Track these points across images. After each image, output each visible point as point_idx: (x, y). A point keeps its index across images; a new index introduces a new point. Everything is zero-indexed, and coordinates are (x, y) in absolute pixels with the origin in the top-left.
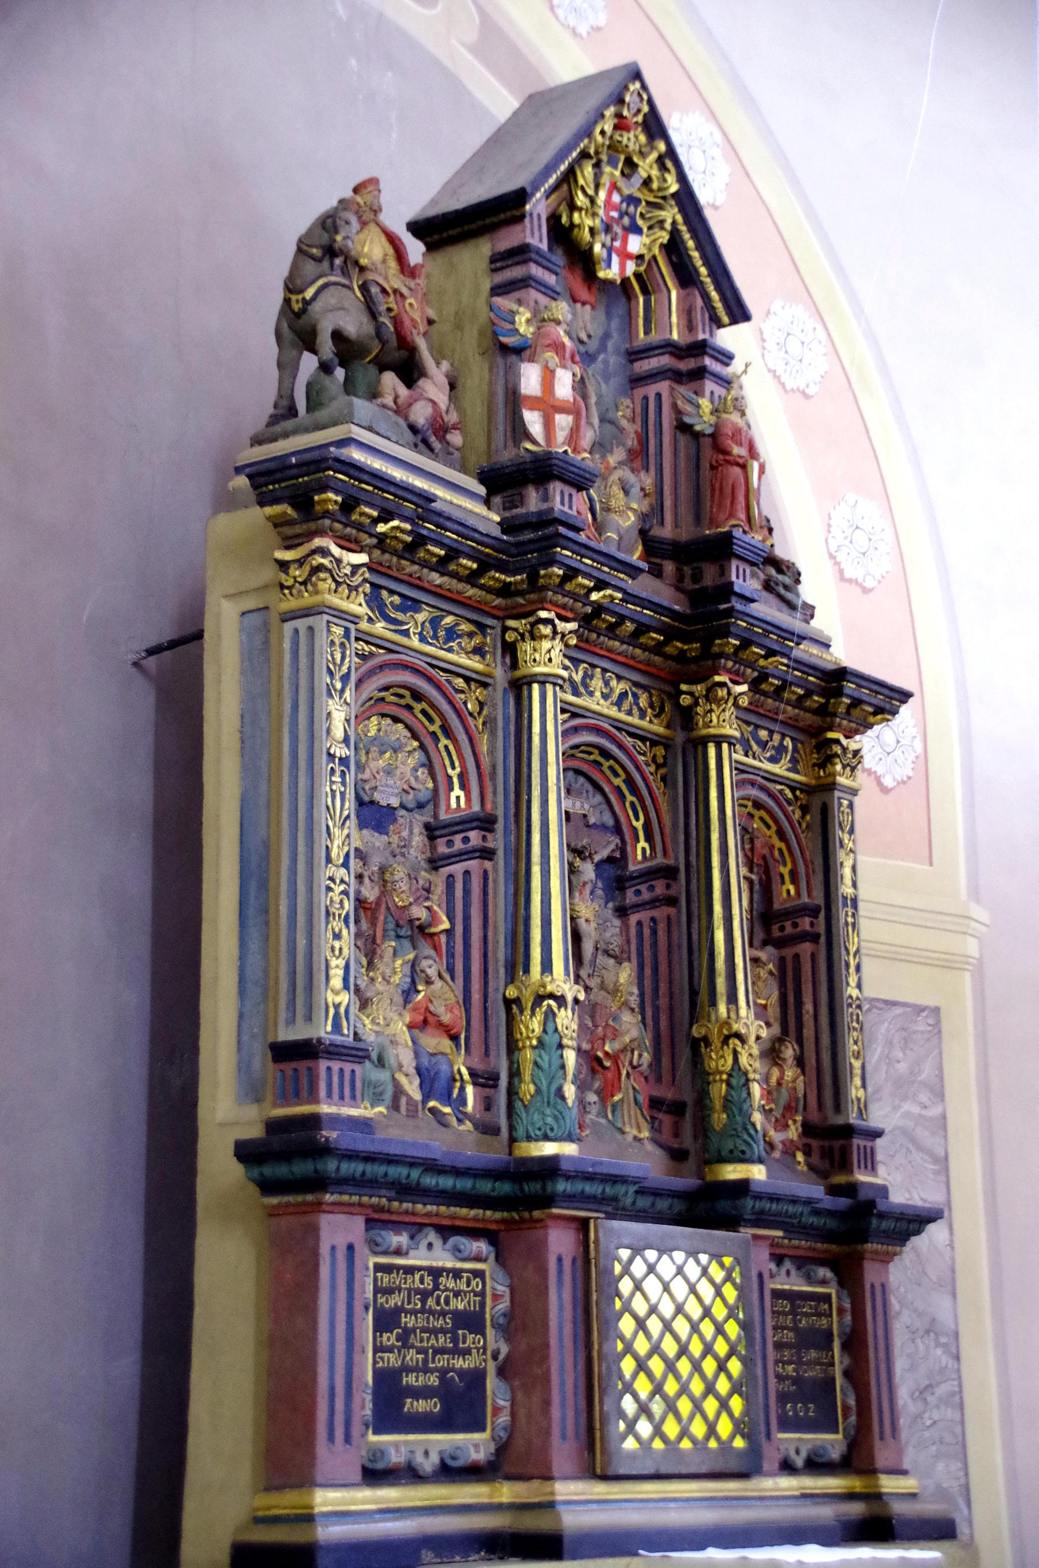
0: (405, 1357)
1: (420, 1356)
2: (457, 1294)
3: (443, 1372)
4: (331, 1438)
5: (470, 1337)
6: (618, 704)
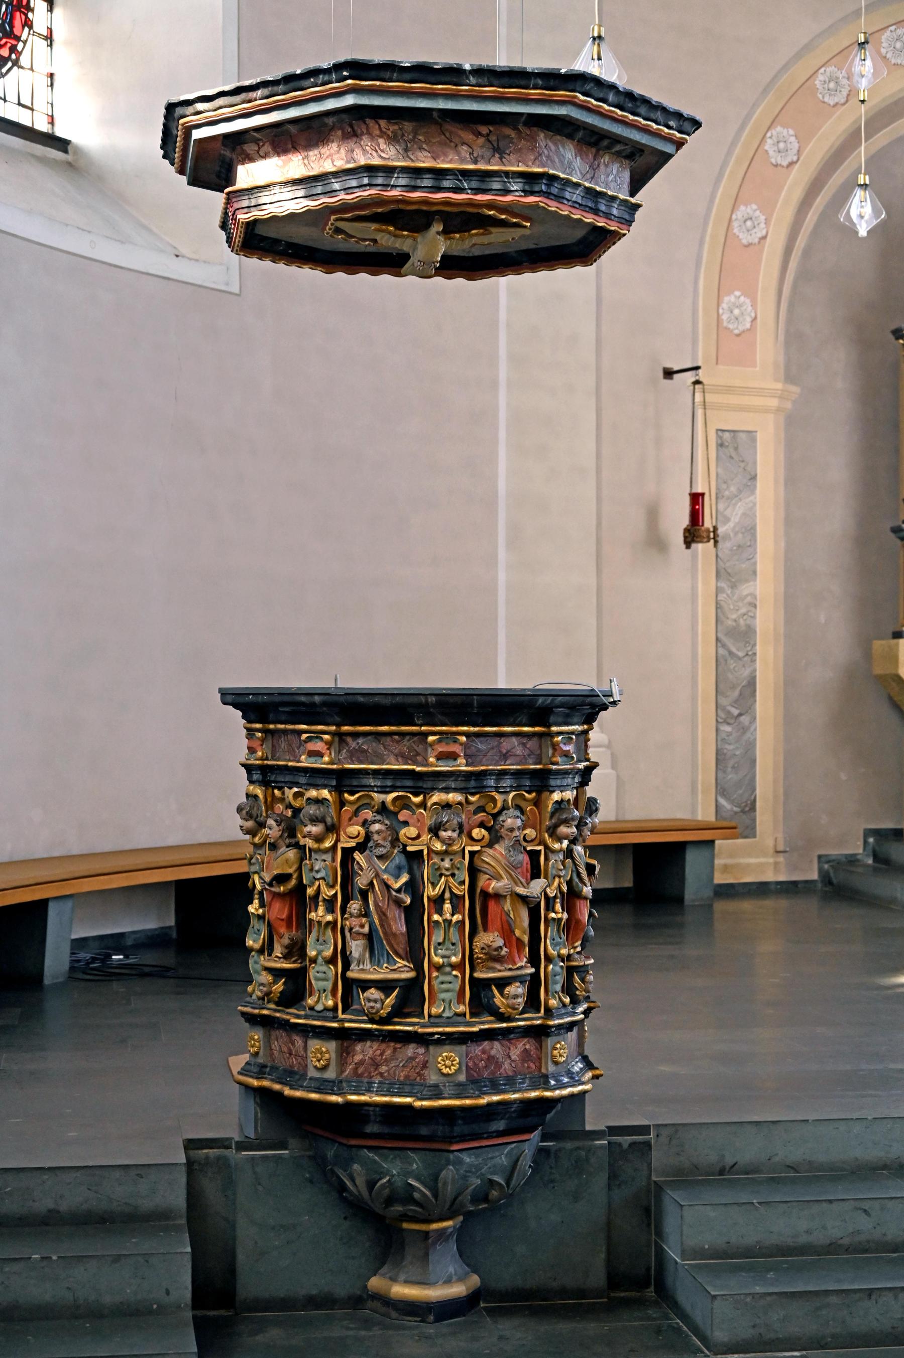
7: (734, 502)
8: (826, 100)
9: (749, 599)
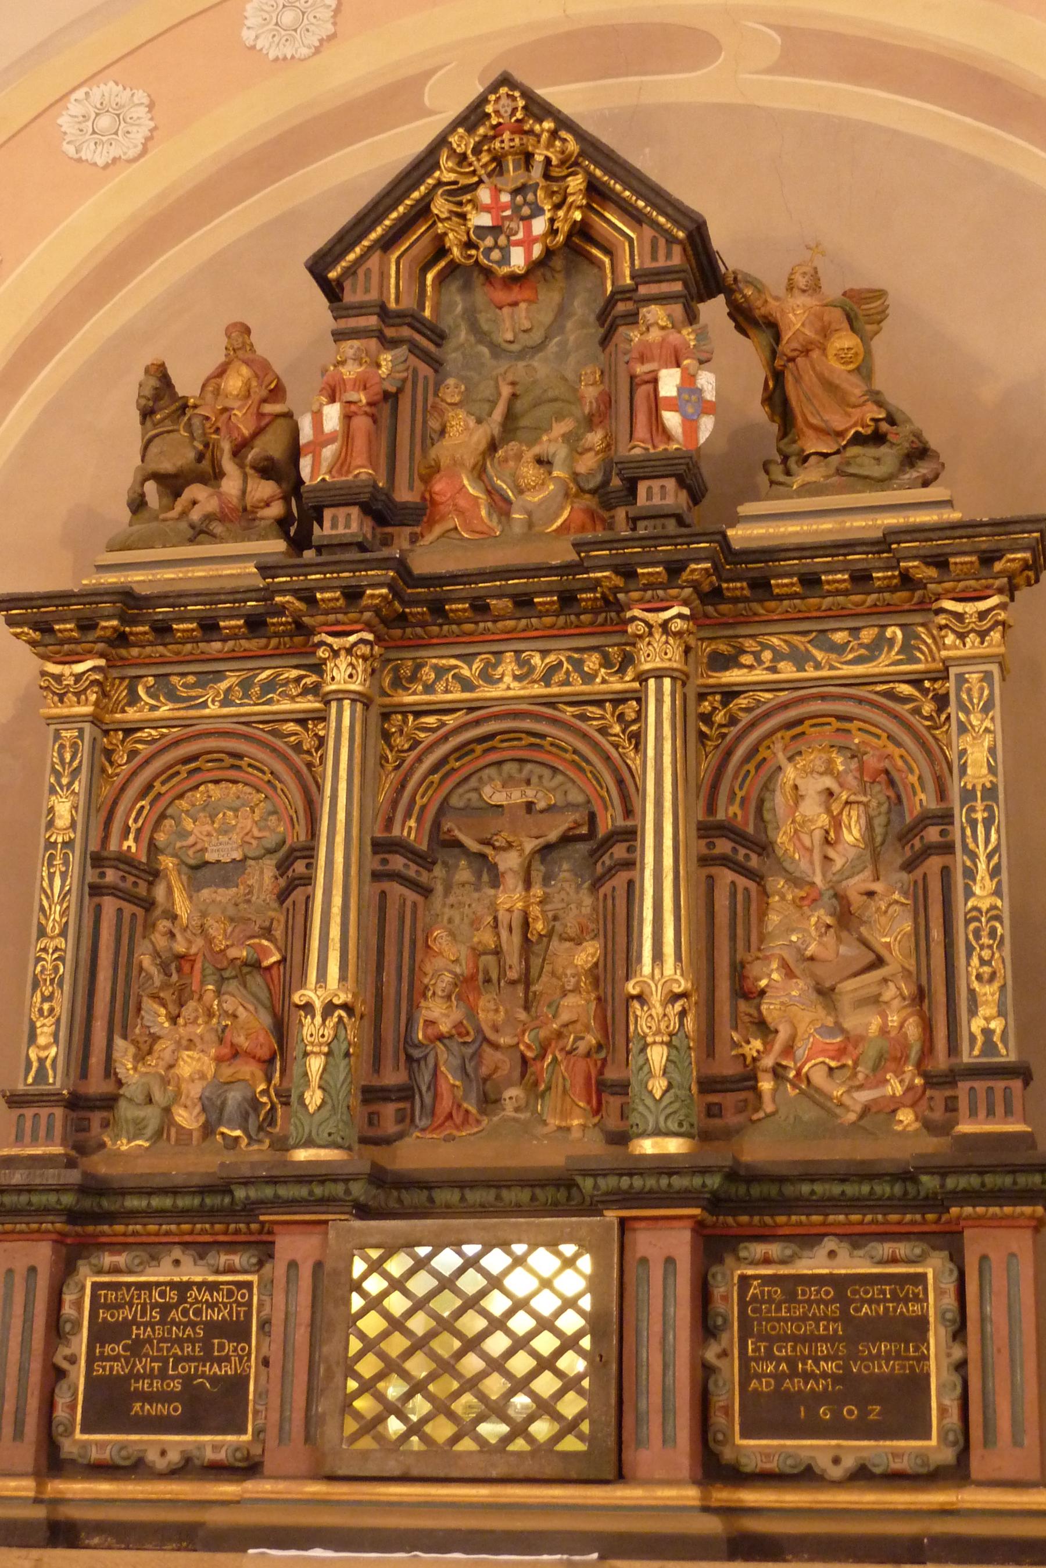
0: (134, 1365)
1: (156, 1365)
2: (212, 1306)
3: (187, 1379)
5: (229, 1347)
6: (546, 679)
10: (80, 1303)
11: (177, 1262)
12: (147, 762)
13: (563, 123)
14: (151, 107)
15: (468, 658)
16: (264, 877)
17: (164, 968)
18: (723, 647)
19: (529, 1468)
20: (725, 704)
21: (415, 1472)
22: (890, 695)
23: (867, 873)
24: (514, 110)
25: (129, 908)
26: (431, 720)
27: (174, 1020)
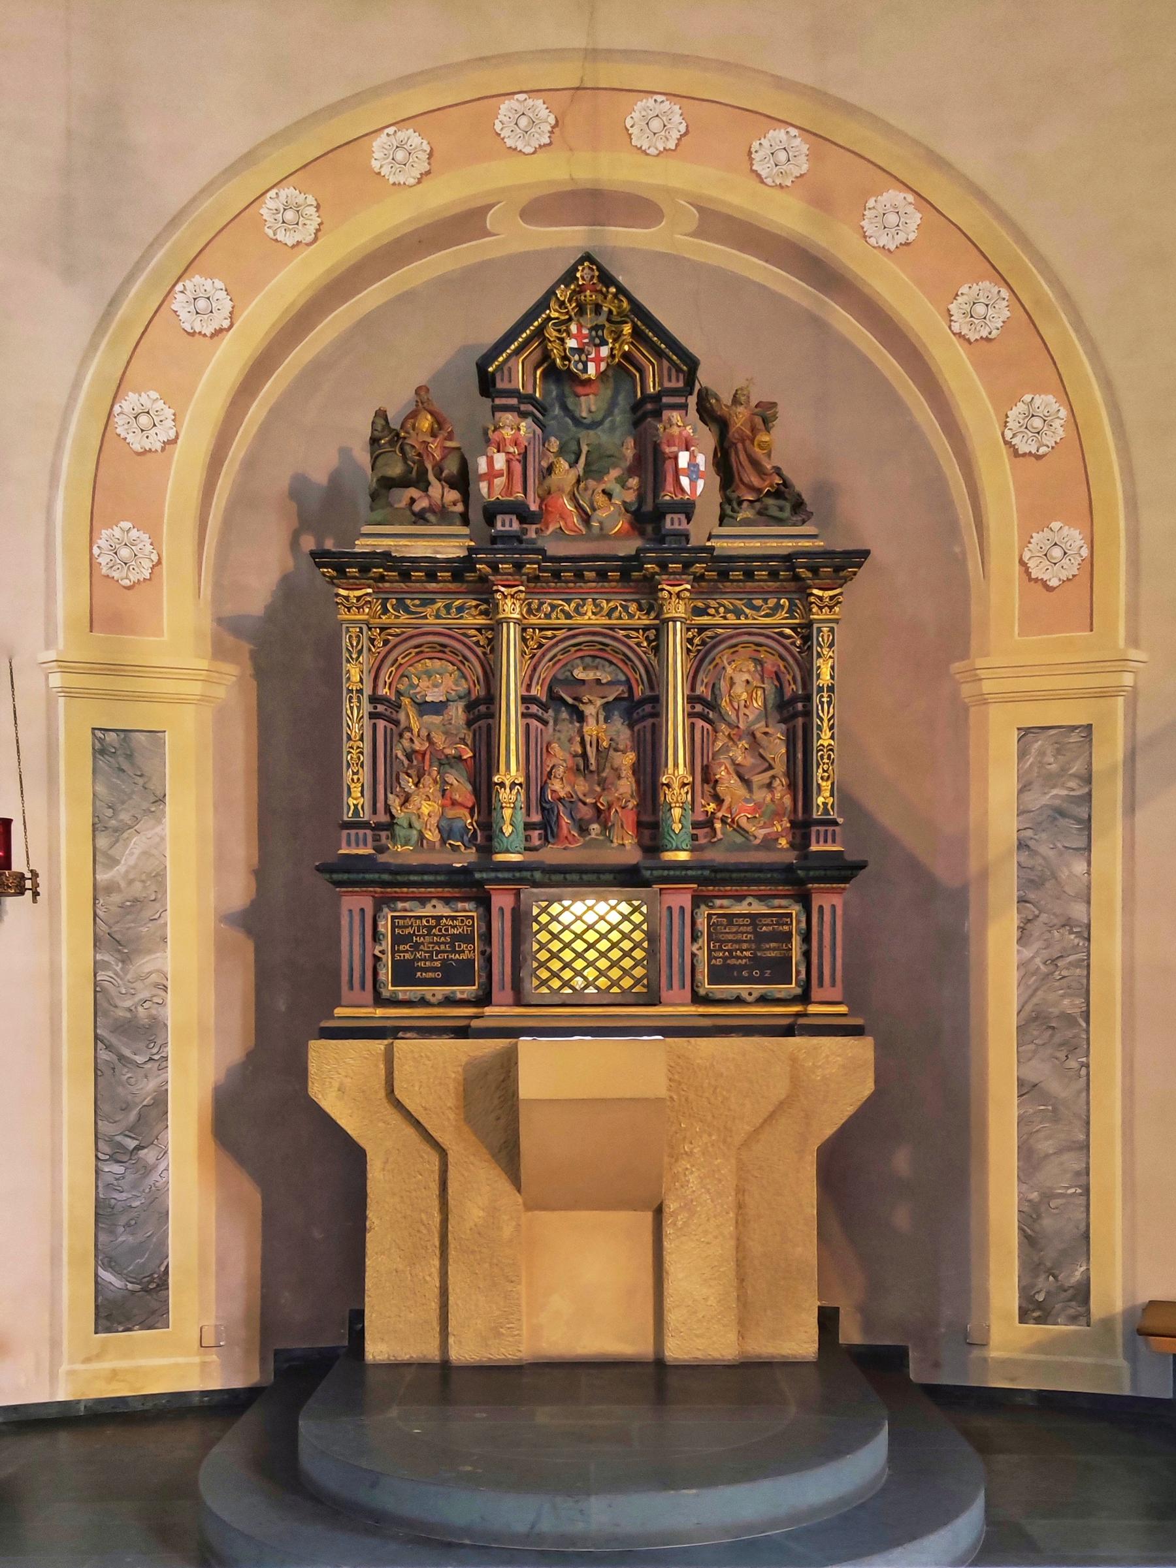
4: (351, 988)
5: (463, 946)
7: (125, 835)
8: (280, 237)
9: (154, 978)
10: (385, 926)
11: (434, 906)
12: (395, 647)
13: (621, 290)
14: (318, 207)
15: (568, 601)
16: (457, 713)
17: (409, 757)
18: (700, 604)
19: (619, 1000)
20: (699, 634)
21: (568, 1002)
22: (781, 634)
23: (763, 723)
24: (593, 277)
25: (389, 726)
26: (549, 633)
27: (416, 785)
